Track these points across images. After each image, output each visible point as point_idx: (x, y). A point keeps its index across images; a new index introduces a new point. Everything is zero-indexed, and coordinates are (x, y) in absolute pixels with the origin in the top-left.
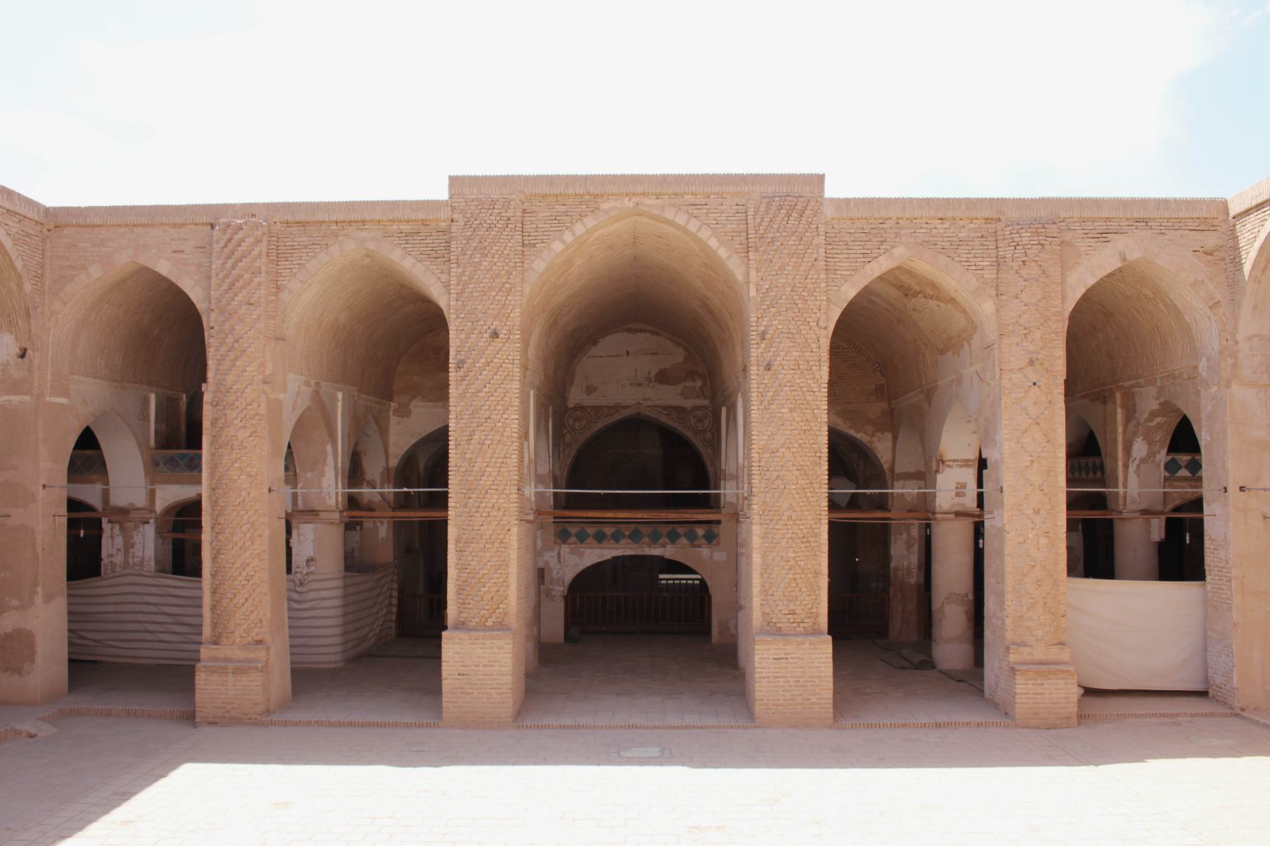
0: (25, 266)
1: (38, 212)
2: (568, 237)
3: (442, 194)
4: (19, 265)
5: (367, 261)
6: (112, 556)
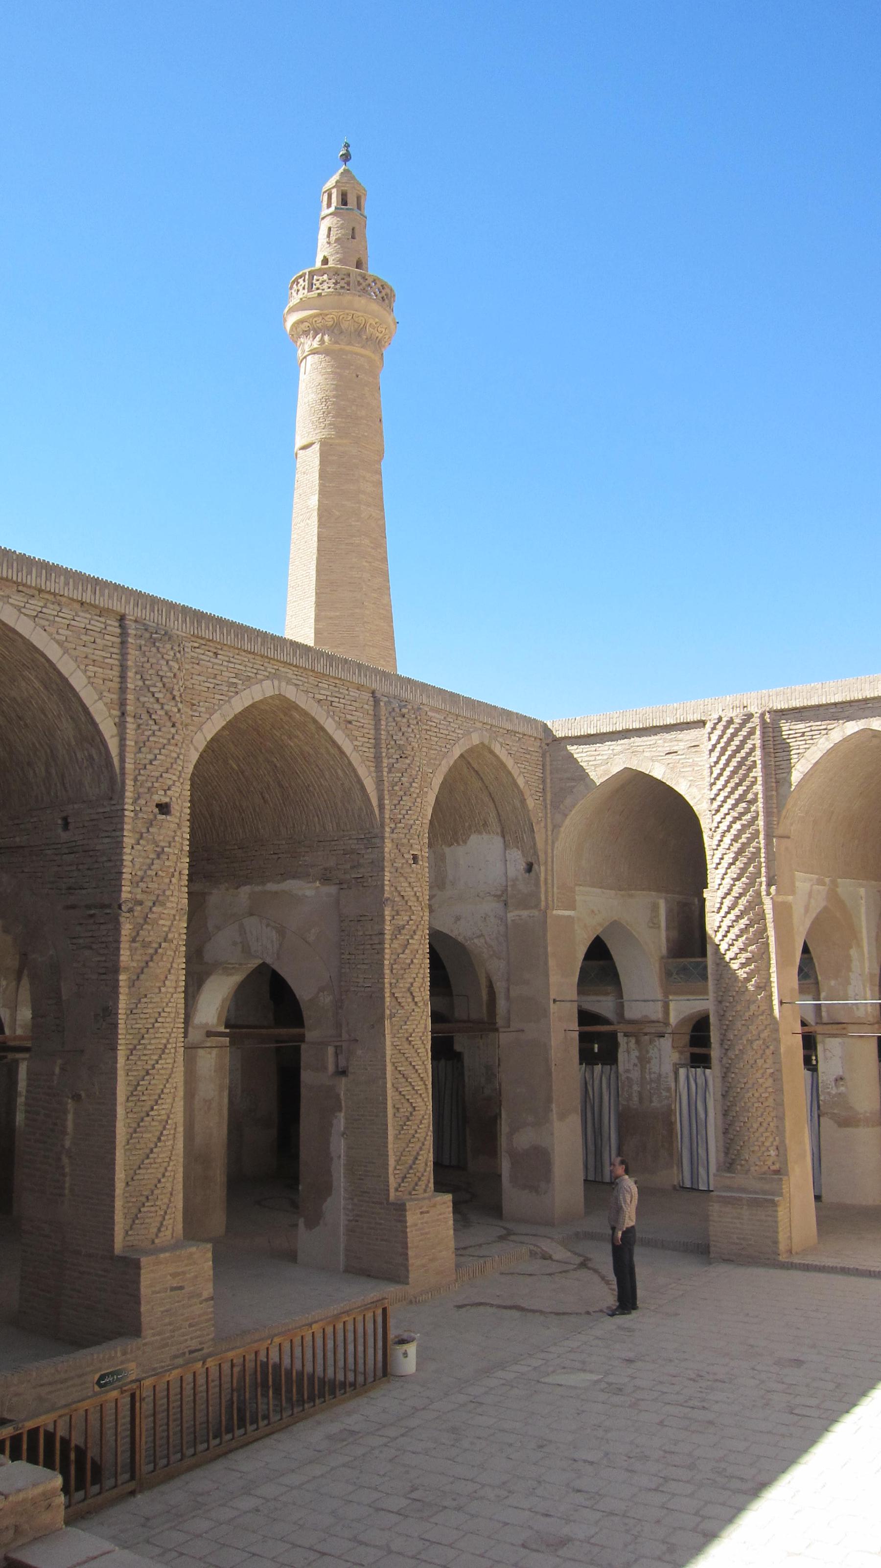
0: (527, 782)
1: (537, 728)
4: (521, 782)
5: (875, 741)
6: (628, 1071)
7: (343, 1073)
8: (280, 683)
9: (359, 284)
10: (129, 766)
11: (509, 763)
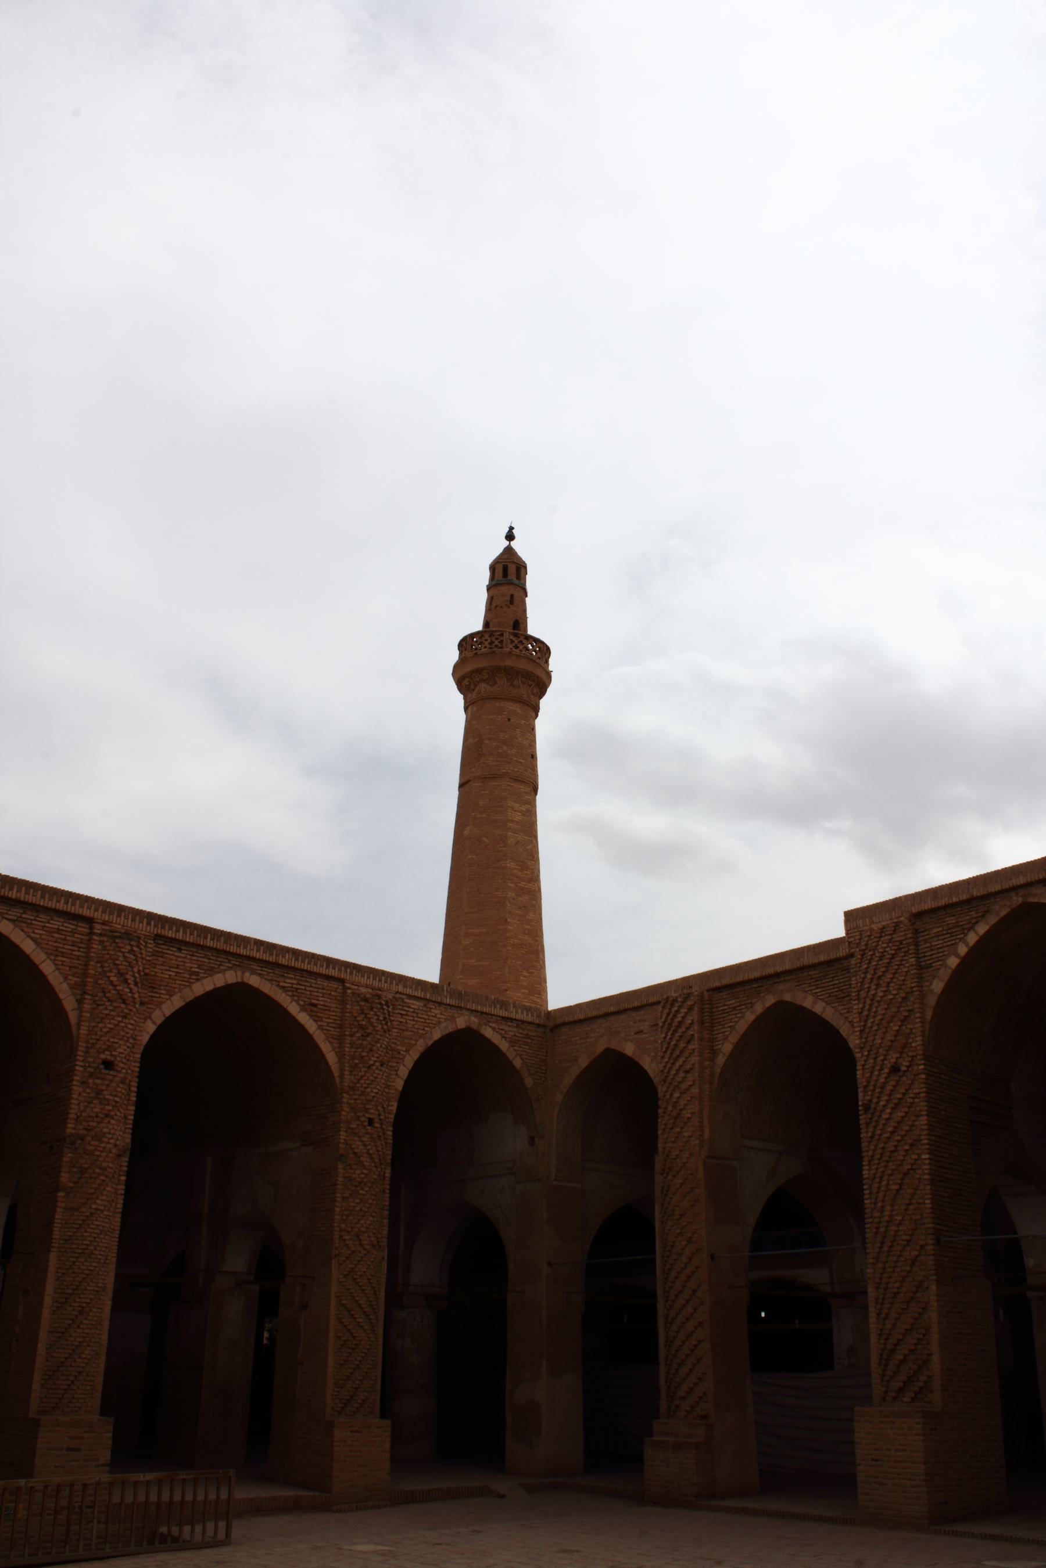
1: (539, 1016)
2: (963, 950)
3: (839, 931)
7: (305, 1307)
8: (243, 973)
9: (512, 642)
10: (84, 1031)
11: (504, 1046)
